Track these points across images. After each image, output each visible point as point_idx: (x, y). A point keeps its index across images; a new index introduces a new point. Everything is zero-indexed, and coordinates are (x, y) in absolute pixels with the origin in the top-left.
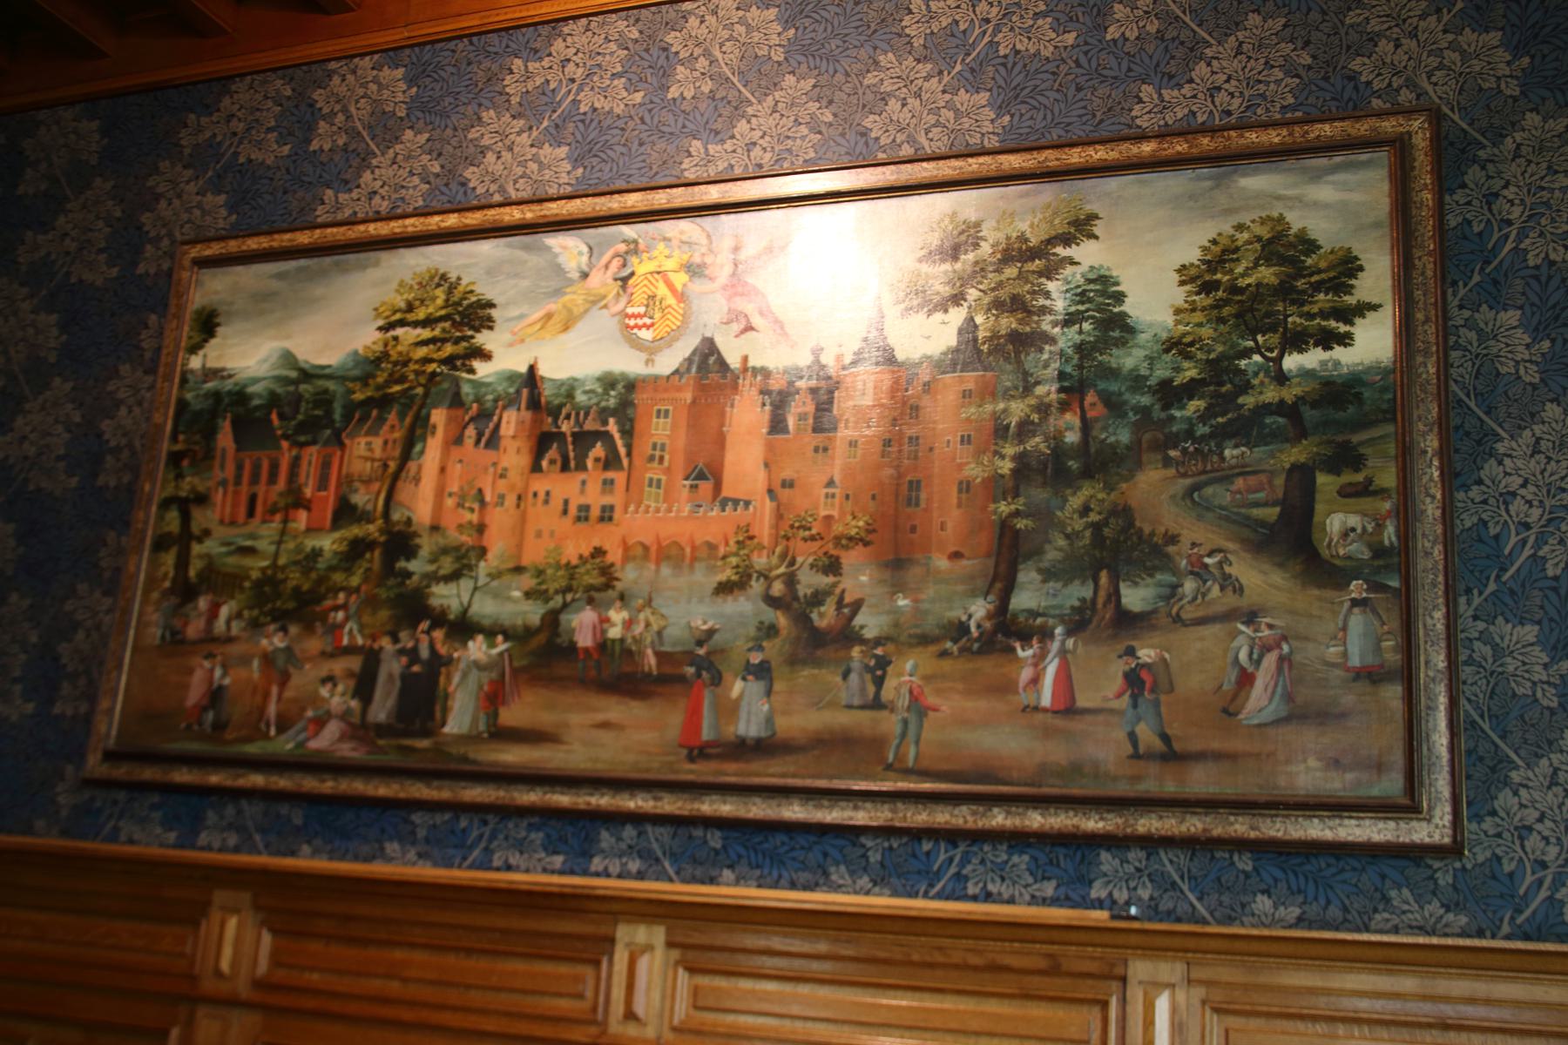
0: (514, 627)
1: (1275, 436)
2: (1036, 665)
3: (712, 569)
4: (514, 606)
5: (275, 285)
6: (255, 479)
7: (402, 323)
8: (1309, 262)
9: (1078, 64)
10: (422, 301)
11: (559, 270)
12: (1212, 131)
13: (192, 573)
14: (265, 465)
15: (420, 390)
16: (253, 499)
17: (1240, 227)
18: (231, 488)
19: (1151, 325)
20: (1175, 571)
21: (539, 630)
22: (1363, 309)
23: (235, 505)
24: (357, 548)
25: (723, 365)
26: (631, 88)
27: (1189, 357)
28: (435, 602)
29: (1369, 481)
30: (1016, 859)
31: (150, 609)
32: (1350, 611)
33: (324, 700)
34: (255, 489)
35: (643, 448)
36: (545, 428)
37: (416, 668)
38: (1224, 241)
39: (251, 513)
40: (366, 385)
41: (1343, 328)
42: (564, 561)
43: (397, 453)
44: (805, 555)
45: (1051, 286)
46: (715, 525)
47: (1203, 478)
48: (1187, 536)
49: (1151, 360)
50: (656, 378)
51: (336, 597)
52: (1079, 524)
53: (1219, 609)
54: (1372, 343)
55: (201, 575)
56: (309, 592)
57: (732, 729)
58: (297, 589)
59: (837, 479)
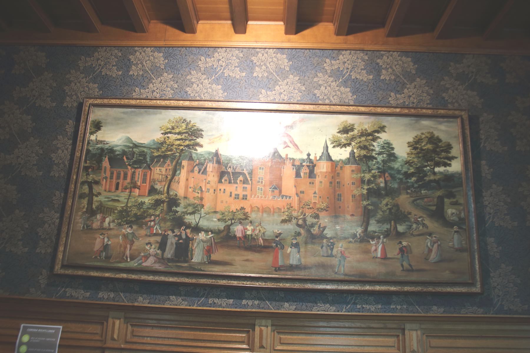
0: (215, 230)
2: (376, 246)
5: (122, 115)
6: (118, 177)
7: (170, 133)
8: (440, 144)
9: (374, 85)
10: (177, 127)
12: (414, 108)
13: (94, 207)
14: (122, 173)
15: (178, 154)
16: (117, 185)
17: (422, 134)
18: (109, 180)
19: (401, 157)
20: (410, 222)
21: (223, 231)
22: (453, 158)
23: (110, 185)
24: (158, 203)
25: (280, 157)
26: (241, 71)
27: (411, 166)
28: (186, 221)
29: (457, 201)
30: (370, 298)
31: (78, 218)
32: (454, 234)
33: (147, 250)
34: (119, 181)
36: (223, 170)
37: (181, 241)
38: (419, 137)
39: (117, 188)
40: (158, 151)
41: (449, 162)
42: (231, 210)
43: (171, 173)
44: (309, 213)
45: (375, 144)
46: (280, 203)
49: (402, 166)
51: (151, 217)
52: (385, 208)
54: (456, 166)
56: (139, 215)
57: (288, 262)
58: (135, 214)
59: (317, 192)
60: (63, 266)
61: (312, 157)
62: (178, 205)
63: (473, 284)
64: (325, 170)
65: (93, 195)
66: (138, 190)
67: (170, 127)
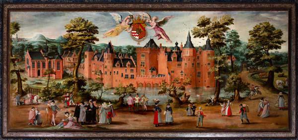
1: (268, 65)
3: (157, 89)
4: (112, 96)
5: (34, 18)
6: (39, 66)
7: (74, 30)
11: (114, 21)
13: (23, 89)
14: (41, 63)
16: (39, 72)
17: (261, 24)
19: (244, 43)
20: (249, 90)
21: (119, 101)
22: (283, 42)
23: (33, 73)
24: (70, 84)
27: (251, 49)
29: (283, 74)
33: (66, 117)
34: (39, 69)
35: (139, 63)
36: (115, 57)
37: (90, 110)
39: (39, 74)
40: (66, 45)
41: (279, 45)
43: (77, 61)
44: (177, 86)
45: (225, 33)
46: (157, 80)
48: (252, 84)
50: (141, 48)
52: (231, 81)
53: (257, 97)
54: (284, 49)
55: (26, 89)
56: (58, 93)
58: (55, 93)
59: (183, 71)
60: (8, 132)
61: (179, 45)
62: (85, 85)
63: (290, 131)
64: (188, 55)
65: (21, 80)
66: (54, 75)
67: (73, 26)
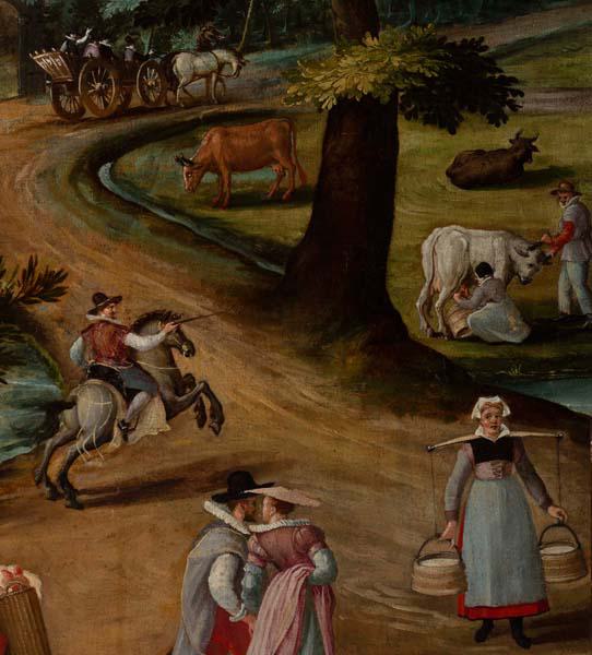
29: (525, 147)
32: (469, 474)
47: (123, 127)
48: (80, 286)
